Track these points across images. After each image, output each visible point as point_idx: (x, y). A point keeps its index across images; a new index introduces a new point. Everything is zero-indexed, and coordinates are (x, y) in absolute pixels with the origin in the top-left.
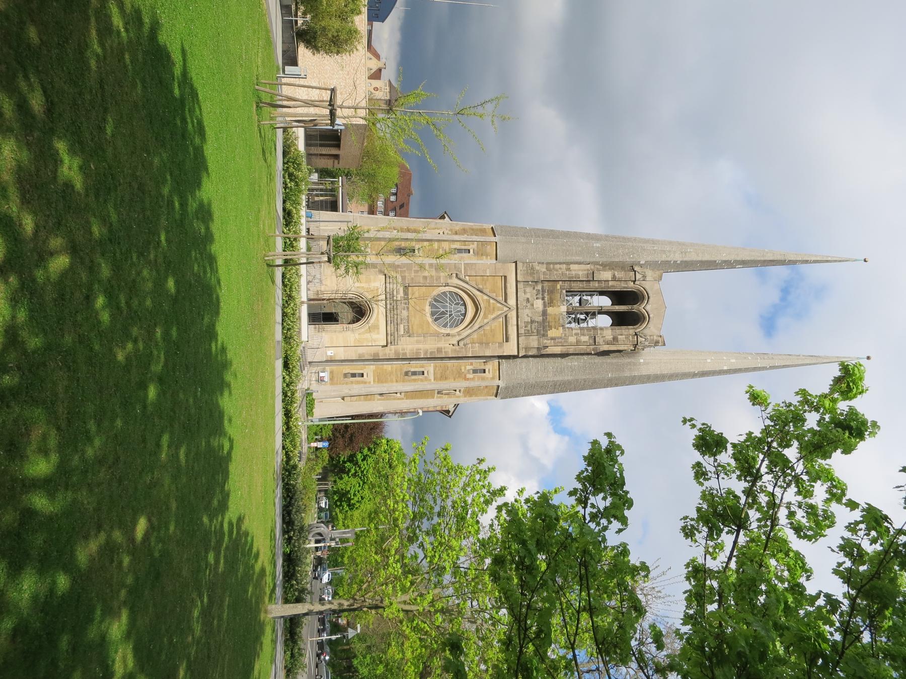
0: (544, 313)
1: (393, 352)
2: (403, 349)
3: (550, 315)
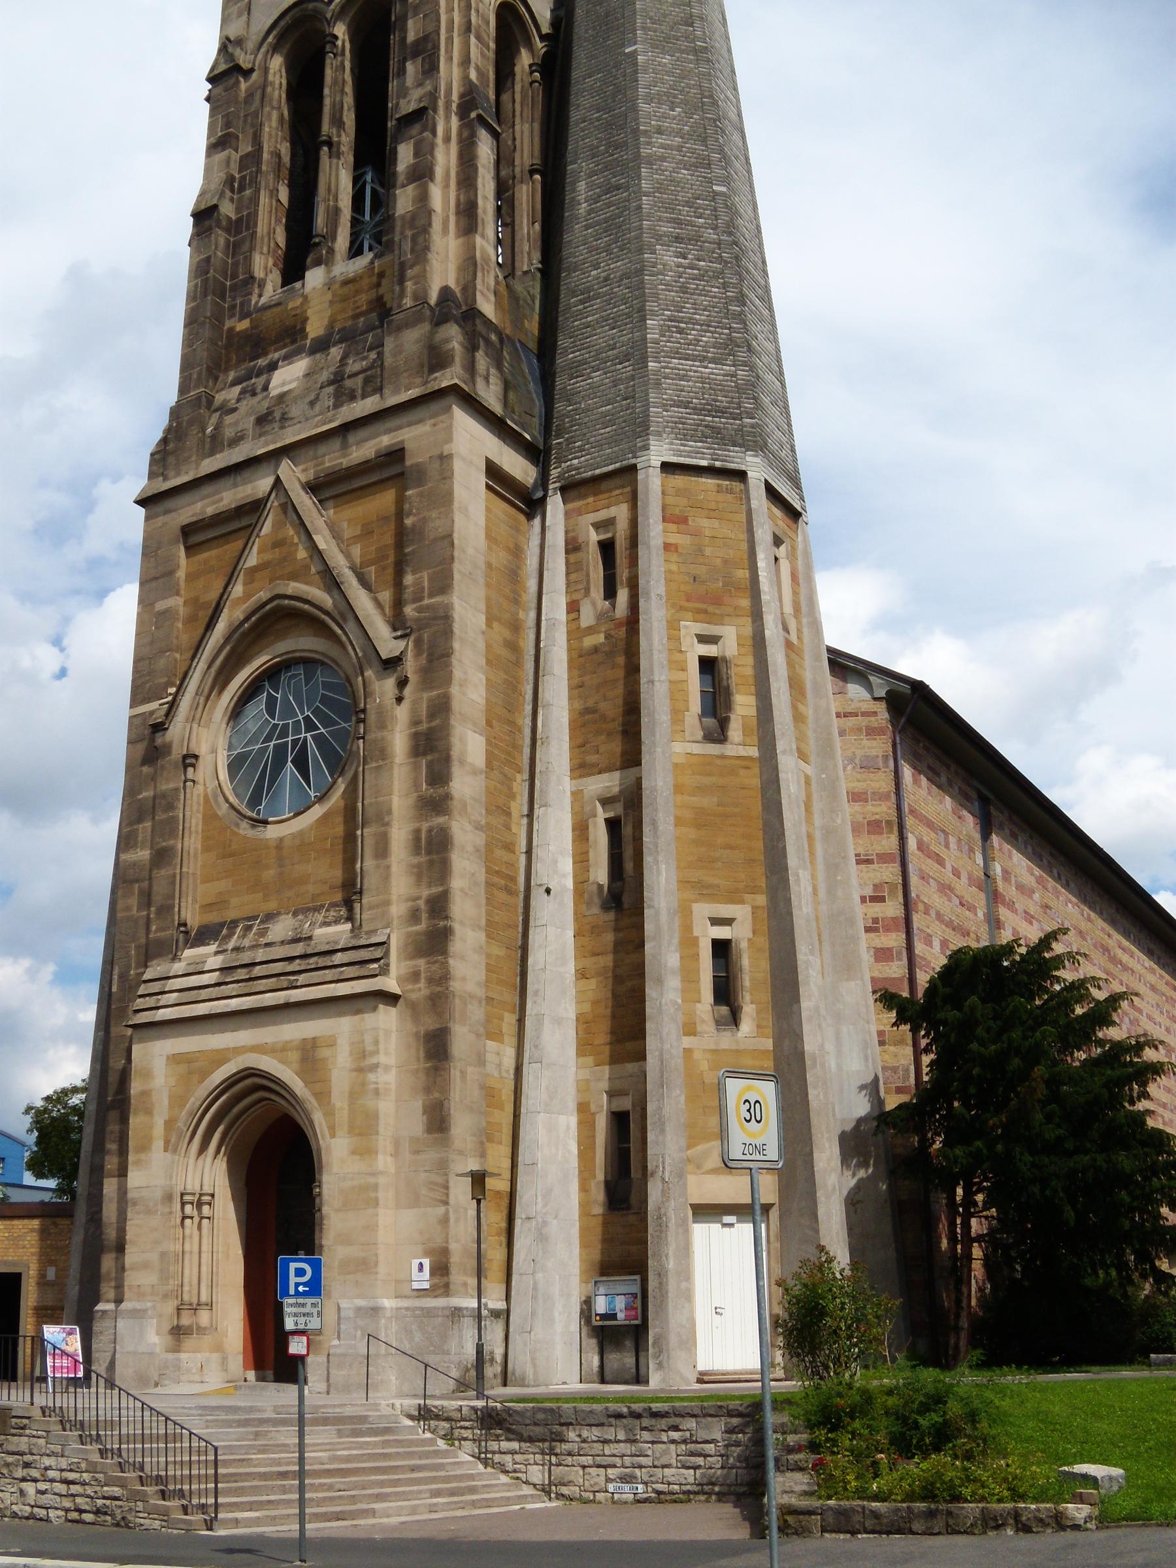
0: (321, 346)
1: (421, 963)
2: (414, 916)
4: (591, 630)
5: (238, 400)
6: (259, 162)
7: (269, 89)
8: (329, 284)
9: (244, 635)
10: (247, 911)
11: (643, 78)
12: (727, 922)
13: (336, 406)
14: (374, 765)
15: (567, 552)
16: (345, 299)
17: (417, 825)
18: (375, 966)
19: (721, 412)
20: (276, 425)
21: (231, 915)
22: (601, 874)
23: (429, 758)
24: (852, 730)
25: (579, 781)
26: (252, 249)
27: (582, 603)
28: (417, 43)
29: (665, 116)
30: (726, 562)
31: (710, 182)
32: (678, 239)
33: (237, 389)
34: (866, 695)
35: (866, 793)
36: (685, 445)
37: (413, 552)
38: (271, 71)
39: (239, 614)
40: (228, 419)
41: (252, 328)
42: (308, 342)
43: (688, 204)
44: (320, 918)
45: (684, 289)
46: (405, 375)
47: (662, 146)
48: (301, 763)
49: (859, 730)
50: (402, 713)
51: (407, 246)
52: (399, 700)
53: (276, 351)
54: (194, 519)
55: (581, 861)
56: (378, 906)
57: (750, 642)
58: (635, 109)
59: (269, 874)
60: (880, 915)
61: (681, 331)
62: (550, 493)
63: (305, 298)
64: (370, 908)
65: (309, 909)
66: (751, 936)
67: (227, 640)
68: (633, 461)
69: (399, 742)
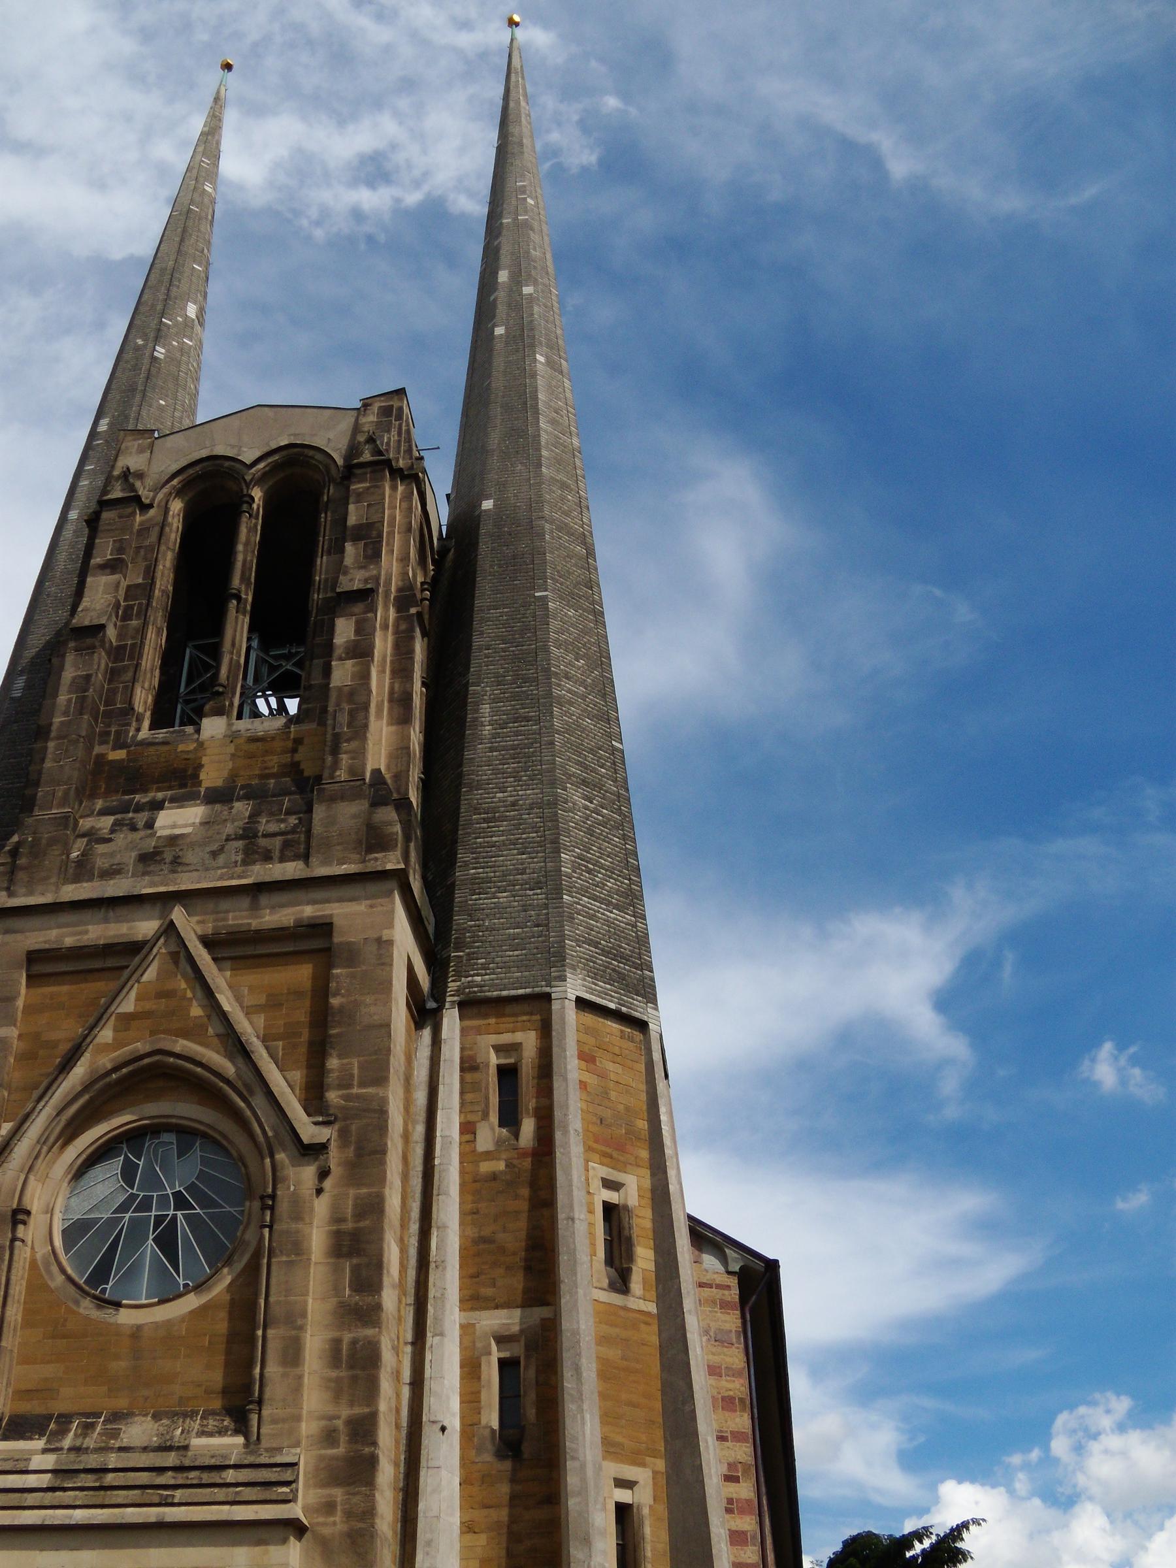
0: (219, 797)
1: (338, 1493)
2: (329, 1437)
3: (233, 777)
4: (488, 1156)
5: (112, 831)
6: (150, 598)
7: (167, 529)
8: (232, 737)
9: (109, 1085)
10: (86, 1405)
11: (554, 624)
12: (628, 1484)
13: (245, 863)
14: (284, 1258)
15: (462, 1070)
16: (251, 756)
17: (337, 1334)
18: (285, 1489)
20: (166, 868)
21: (60, 1406)
22: (492, 1418)
23: (355, 1261)
24: (707, 1301)
25: (472, 1314)
26: (134, 680)
27: (478, 1125)
28: (359, 527)
30: (627, 1109)
32: (584, 782)
33: (110, 820)
34: (720, 1267)
35: (720, 1367)
36: (596, 985)
37: (339, 1035)
38: (171, 513)
39: (106, 1061)
40: (101, 848)
41: (129, 760)
42: (202, 790)
43: (591, 751)
44: (196, 1425)
45: (590, 832)
46: (339, 848)
47: (569, 691)
48: (167, 1242)
49: (714, 1302)
50: (321, 1207)
51: (343, 718)
52: (319, 1191)
53: (159, 790)
54: (47, 946)
55: (471, 1400)
56: (284, 1420)
57: (649, 1195)
58: (546, 650)
59: (120, 1366)
60: (734, 1496)
61: (589, 871)
62: (447, 1005)
63: (201, 745)
64: (274, 1421)
65: (176, 1414)
66: (652, 1502)
67: (86, 1088)
68: (548, 989)
69: (317, 1239)
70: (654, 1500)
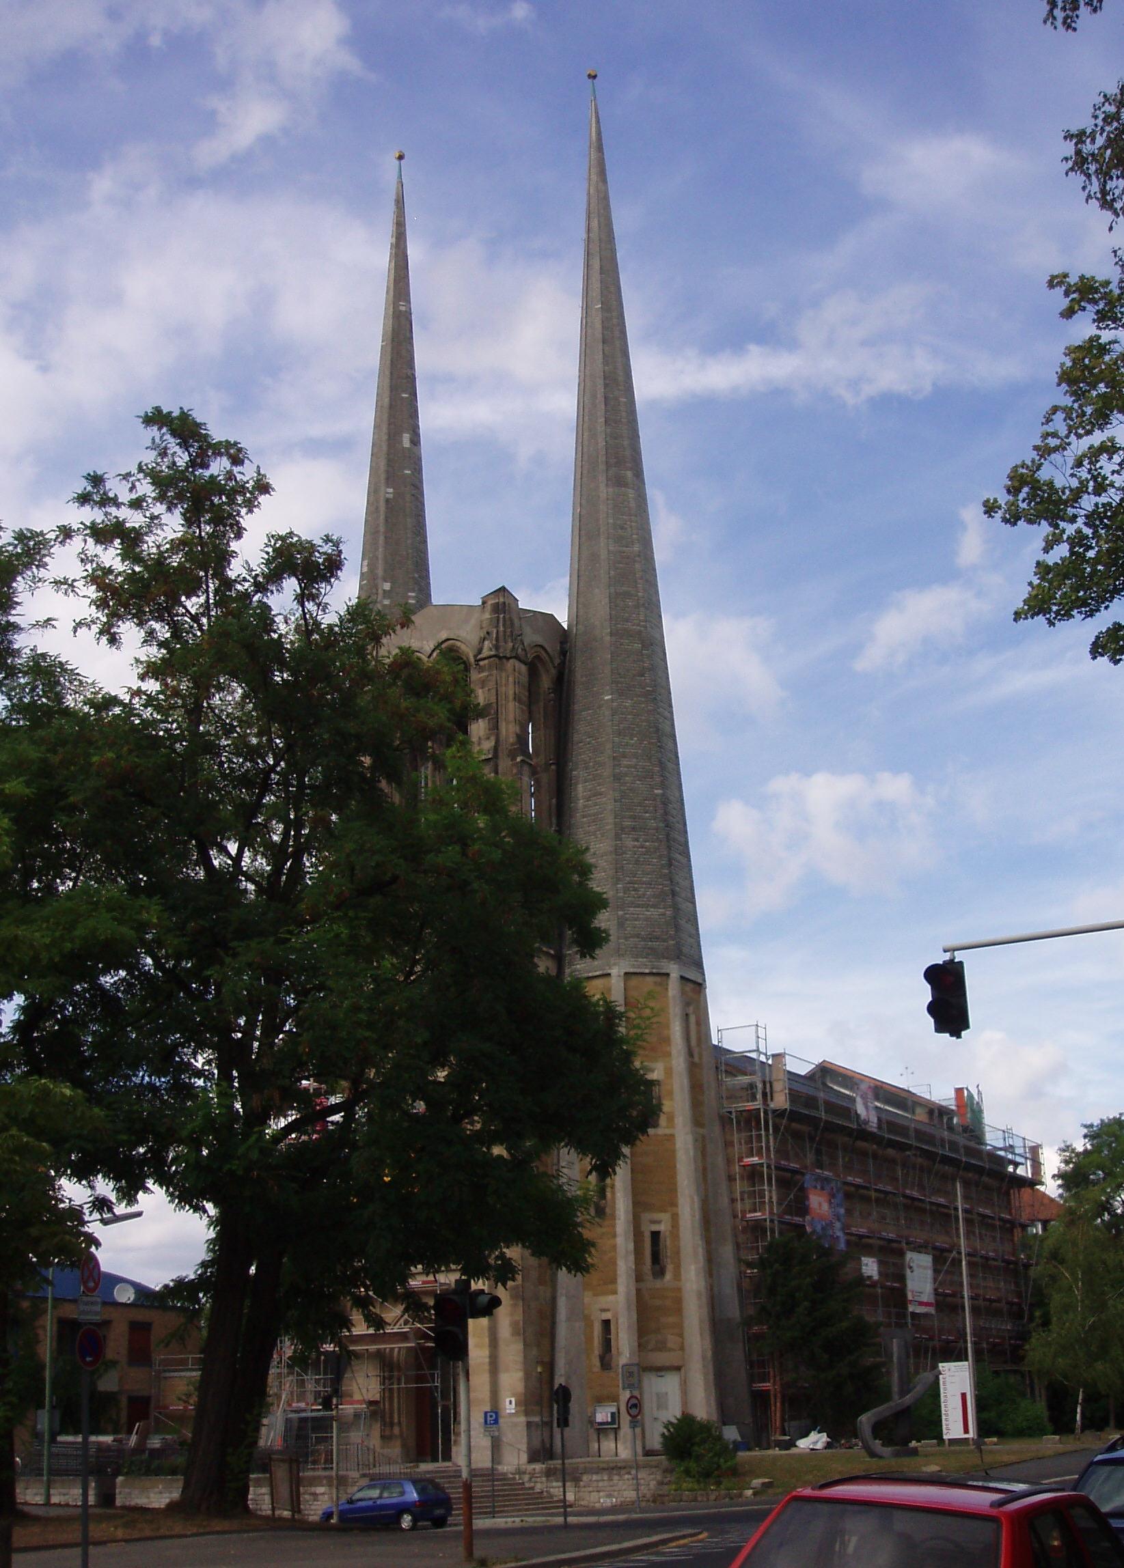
19: (657, 939)
29: (627, 744)
31: (652, 788)
32: (634, 829)
43: (640, 804)
45: (637, 862)
61: (635, 890)
66: (670, 1229)
68: (609, 971)
70: (673, 1227)
